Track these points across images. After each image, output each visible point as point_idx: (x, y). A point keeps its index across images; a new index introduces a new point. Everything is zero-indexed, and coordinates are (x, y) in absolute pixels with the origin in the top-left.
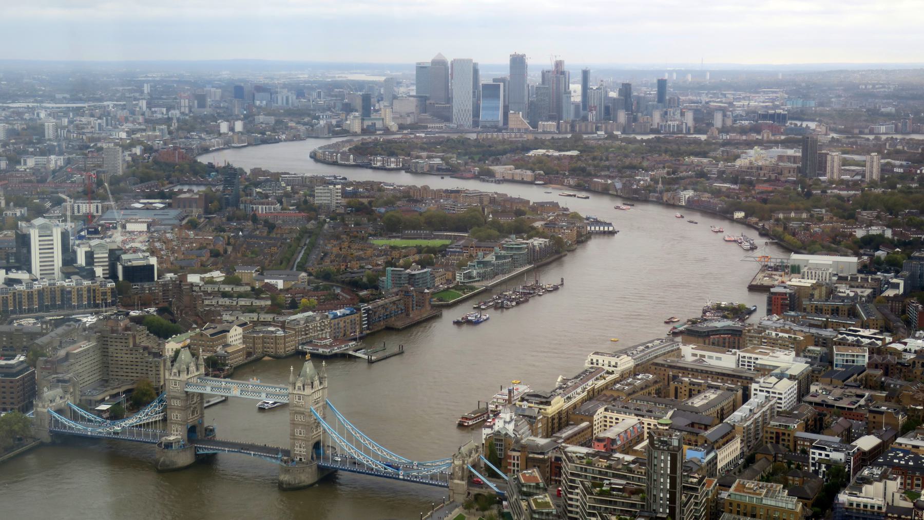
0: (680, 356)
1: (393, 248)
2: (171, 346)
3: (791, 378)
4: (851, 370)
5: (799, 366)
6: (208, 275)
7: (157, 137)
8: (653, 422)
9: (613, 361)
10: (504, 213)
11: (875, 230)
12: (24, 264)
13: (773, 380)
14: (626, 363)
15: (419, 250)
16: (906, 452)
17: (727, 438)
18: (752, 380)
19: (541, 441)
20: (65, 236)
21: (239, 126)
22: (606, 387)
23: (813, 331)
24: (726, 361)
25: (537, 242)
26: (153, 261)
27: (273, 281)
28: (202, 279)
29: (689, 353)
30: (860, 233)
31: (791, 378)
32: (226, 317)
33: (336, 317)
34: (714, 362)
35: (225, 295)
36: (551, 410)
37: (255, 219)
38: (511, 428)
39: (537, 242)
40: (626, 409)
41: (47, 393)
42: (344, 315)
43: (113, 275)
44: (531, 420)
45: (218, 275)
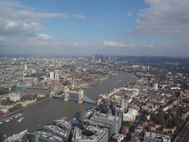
2: (66, 87)
3: (138, 92)
7: (65, 63)
11: (148, 75)
12: (49, 77)
15: (95, 76)
20: (54, 74)
21: (74, 61)
24: (130, 90)
26: (64, 77)
30: (147, 75)
35: (72, 81)
37: (76, 72)
41: (51, 92)
43: (59, 78)
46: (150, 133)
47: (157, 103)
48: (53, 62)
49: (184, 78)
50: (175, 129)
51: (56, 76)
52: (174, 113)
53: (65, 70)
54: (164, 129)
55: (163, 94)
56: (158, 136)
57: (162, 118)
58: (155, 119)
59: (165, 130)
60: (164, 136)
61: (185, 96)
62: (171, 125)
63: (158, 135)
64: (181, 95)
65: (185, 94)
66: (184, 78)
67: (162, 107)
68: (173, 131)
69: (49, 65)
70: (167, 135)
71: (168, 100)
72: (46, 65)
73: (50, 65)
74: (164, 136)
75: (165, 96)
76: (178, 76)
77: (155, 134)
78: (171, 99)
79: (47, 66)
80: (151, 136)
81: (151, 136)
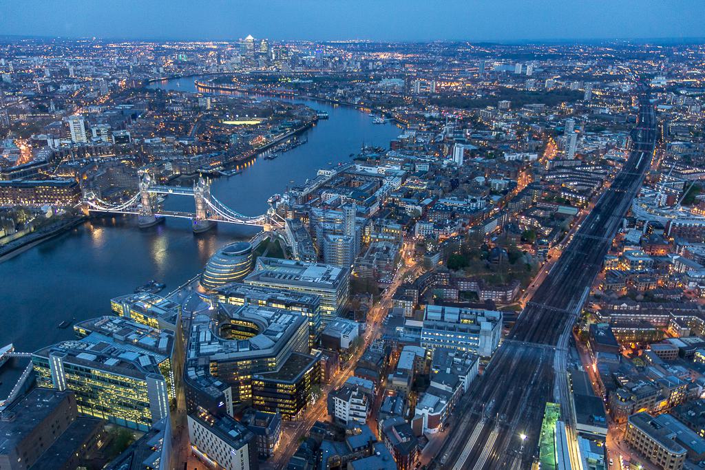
0: (355, 168)
1: (235, 125)
3: (399, 176)
4: (421, 173)
5: (402, 173)
6: (154, 139)
8: (345, 196)
9: (329, 172)
10: (282, 109)
13: (392, 177)
14: (333, 173)
16: (443, 205)
17: (374, 201)
18: (383, 178)
19: (301, 206)
22: (326, 183)
23: (408, 157)
25: (296, 121)
26: (128, 133)
27: (183, 142)
28: (151, 141)
29: (359, 167)
30: (427, 115)
31: (399, 176)
32: (164, 158)
33: (212, 156)
34: (369, 171)
36: (303, 194)
38: (287, 201)
39: (296, 121)
40: (334, 192)
42: (215, 156)
44: (296, 198)
45: (158, 140)
46: (440, 308)
48: (72, 75)
51: (95, 134)
53: (128, 107)
55: (481, 180)
59: (484, 296)
60: (483, 315)
63: (466, 313)
69: (57, 86)
70: (490, 309)
72: (45, 86)
73: (64, 88)
75: (487, 184)
77: (457, 310)
78: (505, 192)
79: (52, 89)
80: (443, 317)
81: (443, 317)
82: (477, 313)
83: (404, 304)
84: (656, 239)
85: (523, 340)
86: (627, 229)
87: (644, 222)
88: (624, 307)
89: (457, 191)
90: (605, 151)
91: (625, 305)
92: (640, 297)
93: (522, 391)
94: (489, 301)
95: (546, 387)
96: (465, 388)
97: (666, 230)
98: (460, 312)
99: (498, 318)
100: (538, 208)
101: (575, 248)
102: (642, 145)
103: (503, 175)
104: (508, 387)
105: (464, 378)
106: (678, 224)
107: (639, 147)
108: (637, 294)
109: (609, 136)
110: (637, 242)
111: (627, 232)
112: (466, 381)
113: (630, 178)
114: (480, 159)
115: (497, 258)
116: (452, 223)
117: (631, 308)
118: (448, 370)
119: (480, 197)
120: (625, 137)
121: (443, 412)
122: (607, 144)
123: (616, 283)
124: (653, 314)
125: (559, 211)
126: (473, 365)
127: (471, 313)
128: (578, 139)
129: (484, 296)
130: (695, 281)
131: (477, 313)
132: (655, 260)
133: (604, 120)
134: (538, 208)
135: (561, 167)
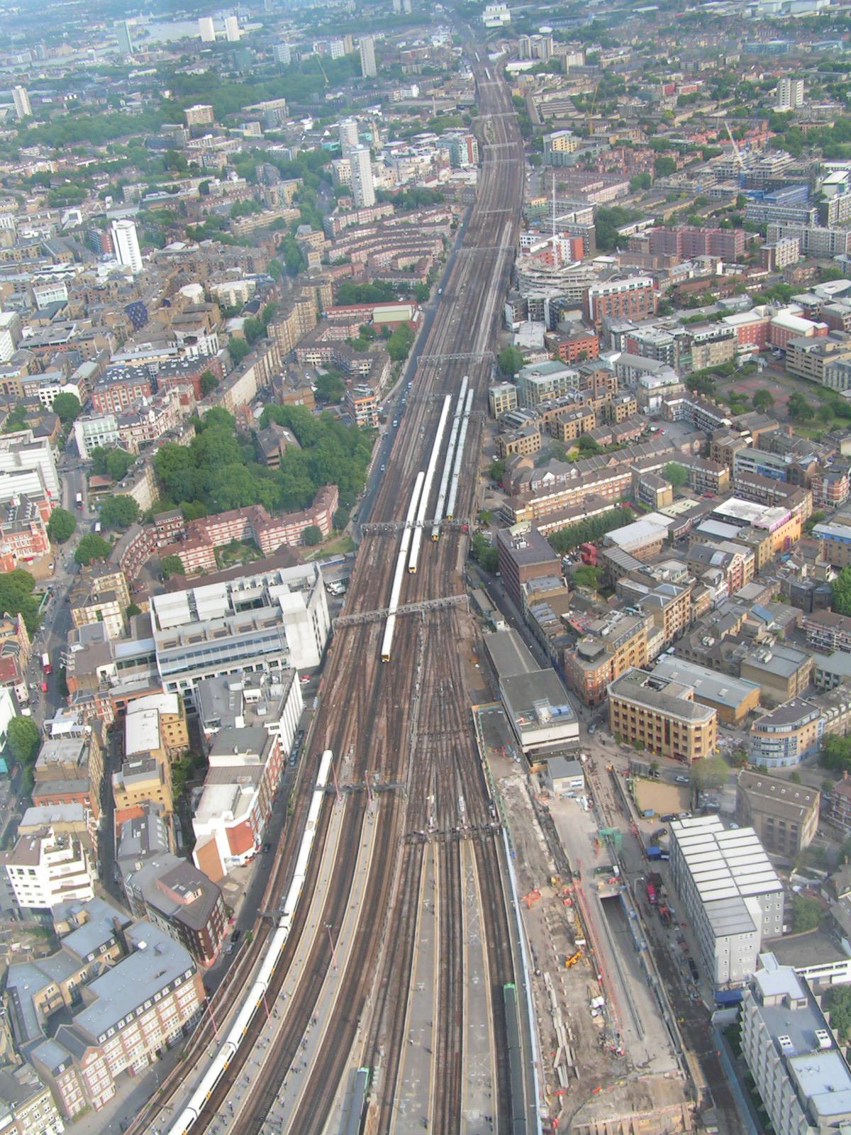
46: (182, 595)
47: (167, 368)
49: (308, 124)
50: (334, 507)
52: (301, 400)
54: (264, 535)
56: (242, 597)
57: (237, 465)
58: (193, 483)
59: (273, 539)
60: (279, 580)
61: (342, 262)
62: (304, 484)
63: (242, 587)
64: (314, 260)
65: (335, 247)
66: (308, 124)
67: (208, 386)
68: (323, 520)
71: (236, 324)
74: (279, 580)
76: (264, 124)
77: (221, 587)
78: (253, 306)
80: (194, 613)
81: (194, 613)
82: (265, 582)
83: (99, 612)
84: (572, 332)
85: (376, 608)
86: (515, 325)
87: (543, 300)
88: (549, 481)
89: (147, 328)
90: (433, 176)
91: (549, 476)
92: (573, 451)
93: (400, 713)
94: (284, 548)
95: (447, 688)
96: (286, 748)
97: (583, 306)
98: (230, 591)
99: (313, 578)
100: (332, 323)
101: (428, 388)
102: (499, 149)
103: (239, 269)
104: (373, 713)
105: (277, 727)
106: (601, 292)
107: (495, 155)
108: (568, 449)
109: (432, 144)
110: (541, 345)
111: (517, 331)
112: (284, 733)
113: (496, 214)
114: (178, 246)
115: (276, 452)
116: (157, 402)
117: (563, 478)
118: (240, 722)
119: (202, 330)
120: (463, 140)
121: (253, 812)
122: (433, 161)
123: (523, 436)
124: (603, 479)
125: (377, 319)
126: (288, 693)
127: (254, 584)
128: (373, 159)
129: (273, 539)
130: (657, 395)
131: (265, 582)
132: (581, 372)
133: (413, 112)
134: (332, 323)
135: (353, 227)
